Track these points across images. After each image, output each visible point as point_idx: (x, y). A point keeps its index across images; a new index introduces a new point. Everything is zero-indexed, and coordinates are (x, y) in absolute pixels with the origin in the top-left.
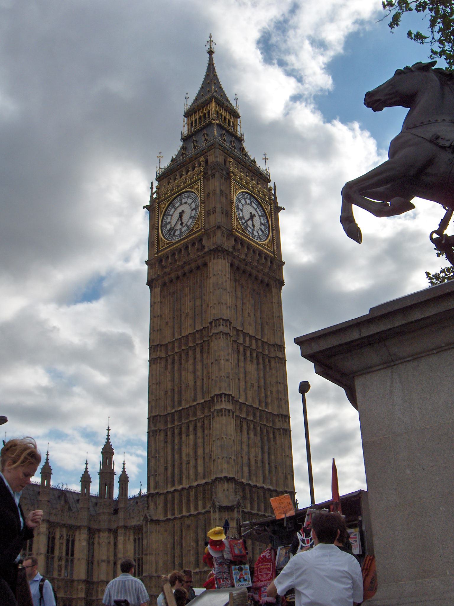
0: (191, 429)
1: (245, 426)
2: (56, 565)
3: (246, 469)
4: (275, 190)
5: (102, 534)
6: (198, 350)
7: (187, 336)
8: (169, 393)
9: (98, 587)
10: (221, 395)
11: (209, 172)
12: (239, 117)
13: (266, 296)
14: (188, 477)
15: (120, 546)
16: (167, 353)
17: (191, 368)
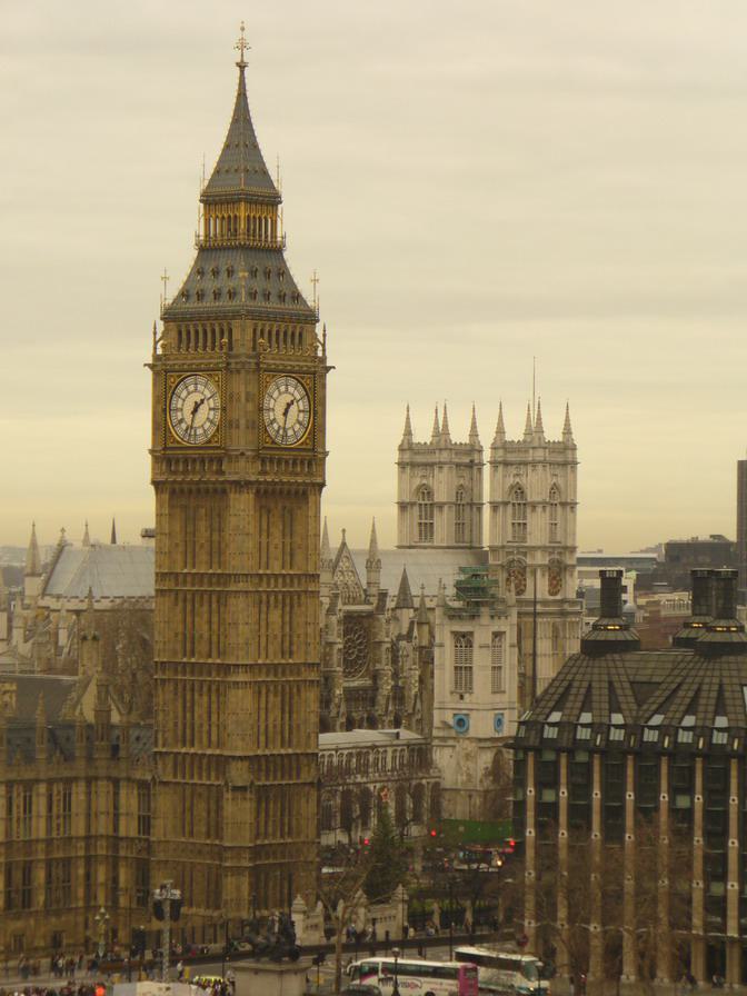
0: (205, 689)
1: (264, 691)
2: (54, 825)
3: (262, 738)
4: (324, 335)
5: (100, 783)
6: (214, 598)
7: (202, 574)
8: (180, 637)
9: (96, 842)
10: (238, 665)
11: (233, 366)
12: (281, 202)
13: (300, 508)
14: (201, 742)
16: (177, 585)
17: (206, 616)
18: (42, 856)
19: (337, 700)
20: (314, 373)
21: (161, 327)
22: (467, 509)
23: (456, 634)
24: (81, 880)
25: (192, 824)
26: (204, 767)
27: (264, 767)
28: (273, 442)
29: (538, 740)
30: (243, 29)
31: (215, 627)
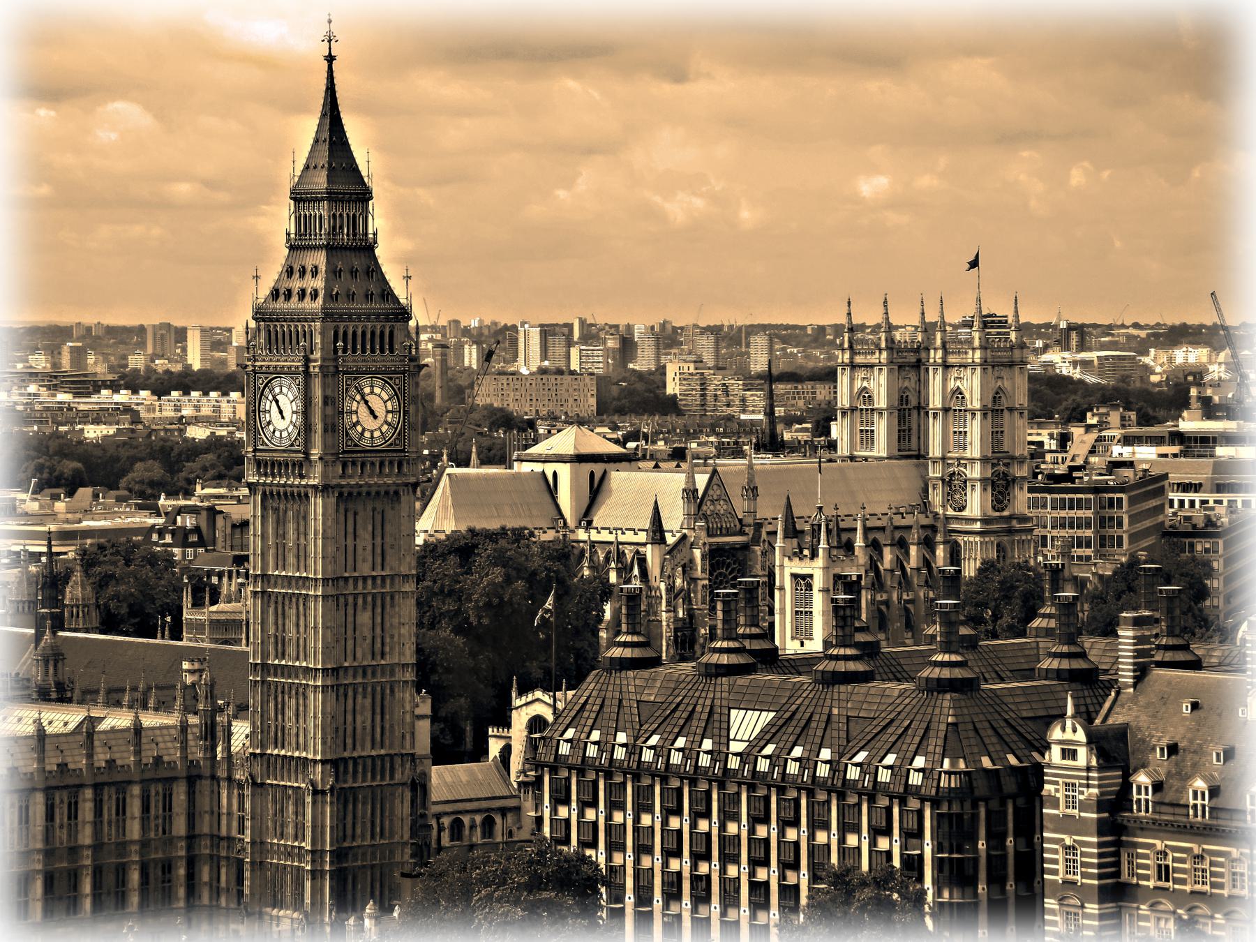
0: (293, 692)
1: (350, 693)
2: (153, 825)
3: (349, 741)
5: (204, 782)
6: (301, 601)
12: (371, 198)
13: (393, 508)
14: (290, 744)
15: (224, 801)
18: (136, 858)
19: (702, 640)
20: (403, 372)
21: (253, 324)
22: (915, 413)
23: (795, 576)
24: (182, 880)
25: (282, 826)
26: (293, 768)
27: (351, 769)
28: (356, 445)
29: (552, 757)
30: (330, 22)
31: (302, 630)
